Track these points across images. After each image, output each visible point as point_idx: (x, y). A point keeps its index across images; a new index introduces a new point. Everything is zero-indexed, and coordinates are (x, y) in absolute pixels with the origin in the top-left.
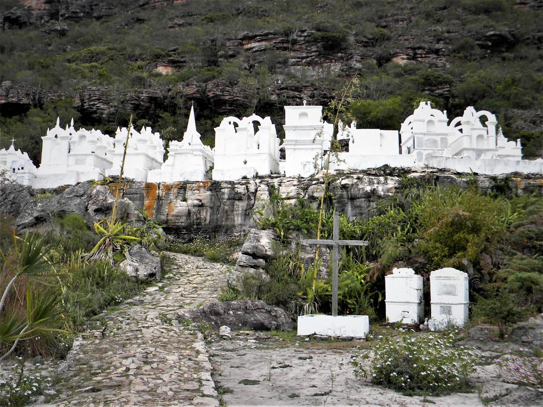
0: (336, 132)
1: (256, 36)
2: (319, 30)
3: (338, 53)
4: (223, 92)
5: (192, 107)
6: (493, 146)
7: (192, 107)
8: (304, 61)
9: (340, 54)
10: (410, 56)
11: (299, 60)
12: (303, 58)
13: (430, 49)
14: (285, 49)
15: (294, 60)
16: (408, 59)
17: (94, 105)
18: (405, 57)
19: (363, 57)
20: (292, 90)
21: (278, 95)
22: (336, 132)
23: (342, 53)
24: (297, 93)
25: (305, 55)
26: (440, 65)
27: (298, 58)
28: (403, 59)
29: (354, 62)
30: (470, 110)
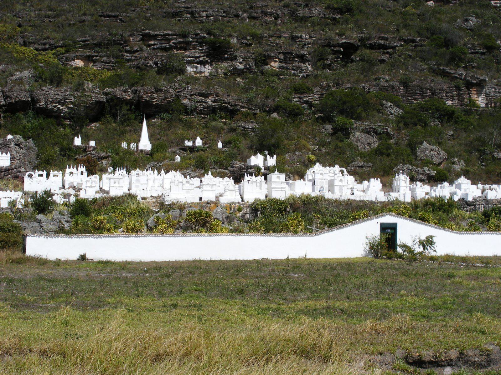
0: (265, 160)
1: (157, 35)
2: (209, 33)
3: (225, 54)
4: (152, 99)
5: (145, 119)
6: (346, 184)
7: (145, 119)
8: (197, 60)
9: (226, 56)
10: (281, 59)
11: (193, 59)
12: (196, 57)
13: (296, 54)
14: (180, 49)
15: (189, 59)
16: (280, 62)
17: (55, 106)
18: (277, 60)
19: (245, 59)
20: (200, 96)
21: (189, 99)
22: (265, 160)
23: (228, 55)
24: (203, 98)
25: (198, 55)
26: (304, 68)
27: (193, 57)
28: (276, 62)
29: (238, 64)
30: (337, 166)
